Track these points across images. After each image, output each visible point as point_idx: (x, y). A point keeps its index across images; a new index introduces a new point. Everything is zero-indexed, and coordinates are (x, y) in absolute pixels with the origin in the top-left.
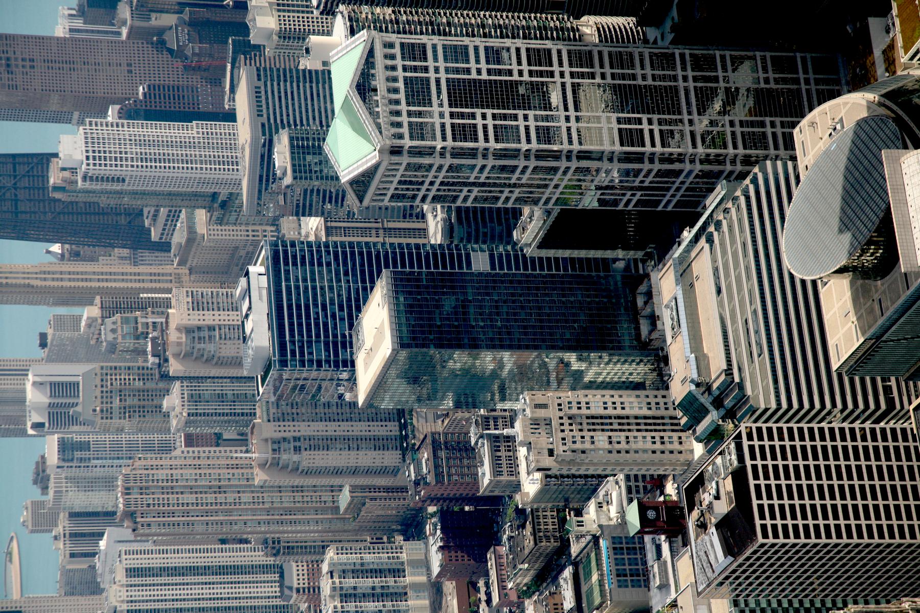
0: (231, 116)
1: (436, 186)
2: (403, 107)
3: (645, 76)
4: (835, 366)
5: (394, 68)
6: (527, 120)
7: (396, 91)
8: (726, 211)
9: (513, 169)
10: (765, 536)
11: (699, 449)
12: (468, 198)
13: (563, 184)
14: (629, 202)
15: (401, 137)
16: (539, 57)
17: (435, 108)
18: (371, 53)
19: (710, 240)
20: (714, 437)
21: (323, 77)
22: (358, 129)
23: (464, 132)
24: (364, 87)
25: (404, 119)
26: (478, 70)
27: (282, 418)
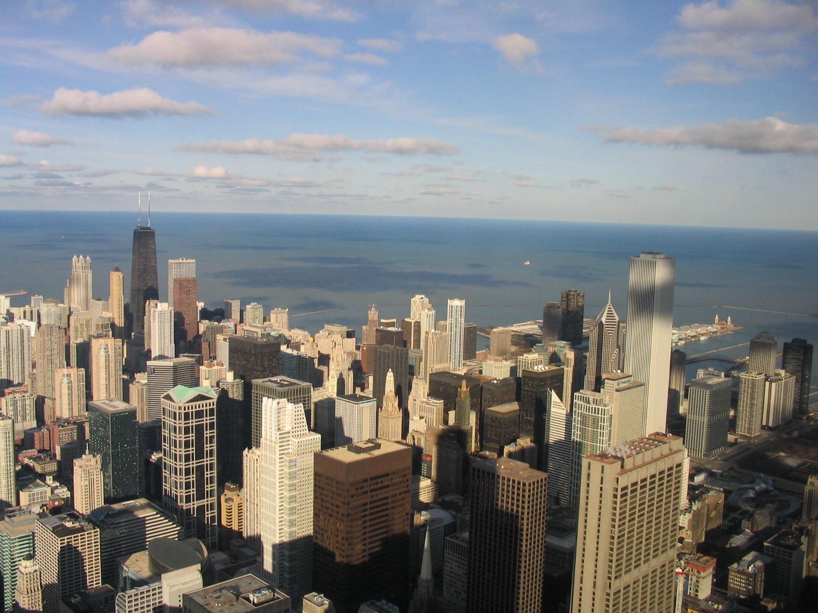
1: (169, 422)
2: (194, 410)
3: (208, 488)
4: (118, 559)
5: (206, 406)
6: (192, 450)
7: (199, 407)
8: (165, 519)
9: (175, 446)
10: (61, 540)
12: (165, 432)
13: (171, 464)
15: (185, 409)
17: (194, 420)
18: (211, 398)
19: (157, 514)
26: (207, 434)
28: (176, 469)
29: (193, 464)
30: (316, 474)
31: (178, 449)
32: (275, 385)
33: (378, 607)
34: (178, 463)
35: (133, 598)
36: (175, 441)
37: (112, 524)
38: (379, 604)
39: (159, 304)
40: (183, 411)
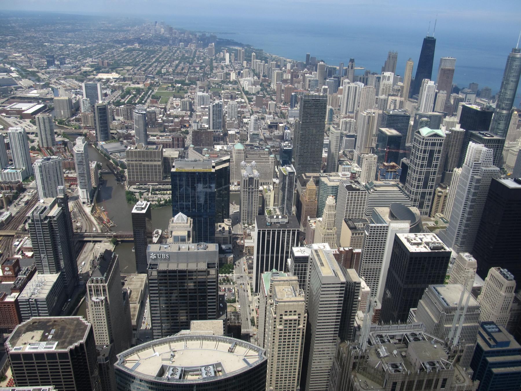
0: (433, 111)
2: (431, 141)
3: (430, 183)
6: (425, 162)
9: (417, 159)
11: (364, 184)
12: (413, 151)
14: (408, 178)
16: (436, 165)
20: (366, 187)
21: (438, 128)
22: (428, 133)
23: (425, 152)
24: (436, 135)
25: (429, 141)
26: (436, 155)
27: (379, 114)
28: (415, 170)
29: (424, 170)
30: (490, 190)
31: (418, 160)
32: (481, 136)
33: (501, 271)
34: (417, 167)
35: (373, 228)
36: (417, 156)
37: (376, 191)
38: (502, 270)
39: (429, 82)
40: (425, 141)
